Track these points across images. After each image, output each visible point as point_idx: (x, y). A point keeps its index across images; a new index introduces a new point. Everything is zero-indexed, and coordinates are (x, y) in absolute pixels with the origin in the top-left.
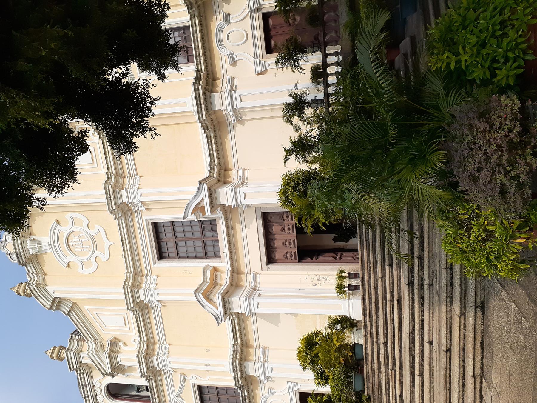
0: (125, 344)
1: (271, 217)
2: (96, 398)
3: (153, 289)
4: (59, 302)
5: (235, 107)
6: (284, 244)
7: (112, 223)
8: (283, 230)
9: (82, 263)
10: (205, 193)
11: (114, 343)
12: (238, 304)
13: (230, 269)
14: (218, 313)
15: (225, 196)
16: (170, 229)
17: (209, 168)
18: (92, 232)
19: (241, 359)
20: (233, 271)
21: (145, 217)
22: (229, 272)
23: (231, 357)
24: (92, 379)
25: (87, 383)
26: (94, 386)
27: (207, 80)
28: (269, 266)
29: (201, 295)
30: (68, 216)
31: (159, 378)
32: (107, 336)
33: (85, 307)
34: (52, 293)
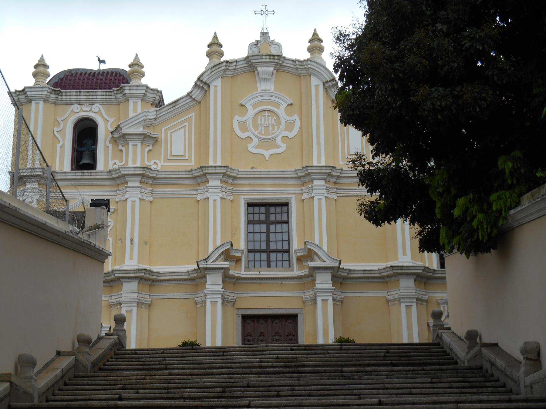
0: (150, 151)
1: (290, 323)
2: (77, 103)
3: (221, 195)
4: (203, 88)
5: (402, 301)
6: (262, 334)
7: (294, 166)
8: (277, 334)
9: (245, 122)
10: (329, 263)
11: (149, 139)
12: (214, 284)
13: (242, 276)
14: (210, 262)
15: (324, 282)
16: (279, 218)
17: (347, 267)
18: (278, 140)
19: (141, 278)
20: (238, 279)
21: (294, 196)
22: (239, 275)
23: (148, 269)
24: (102, 104)
25: (98, 97)
26: (92, 104)
27: (425, 277)
28: (241, 316)
29: (228, 247)
30: (296, 117)
31: (107, 182)
32: (161, 133)
33: (193, 114)
34: (215, 83)
